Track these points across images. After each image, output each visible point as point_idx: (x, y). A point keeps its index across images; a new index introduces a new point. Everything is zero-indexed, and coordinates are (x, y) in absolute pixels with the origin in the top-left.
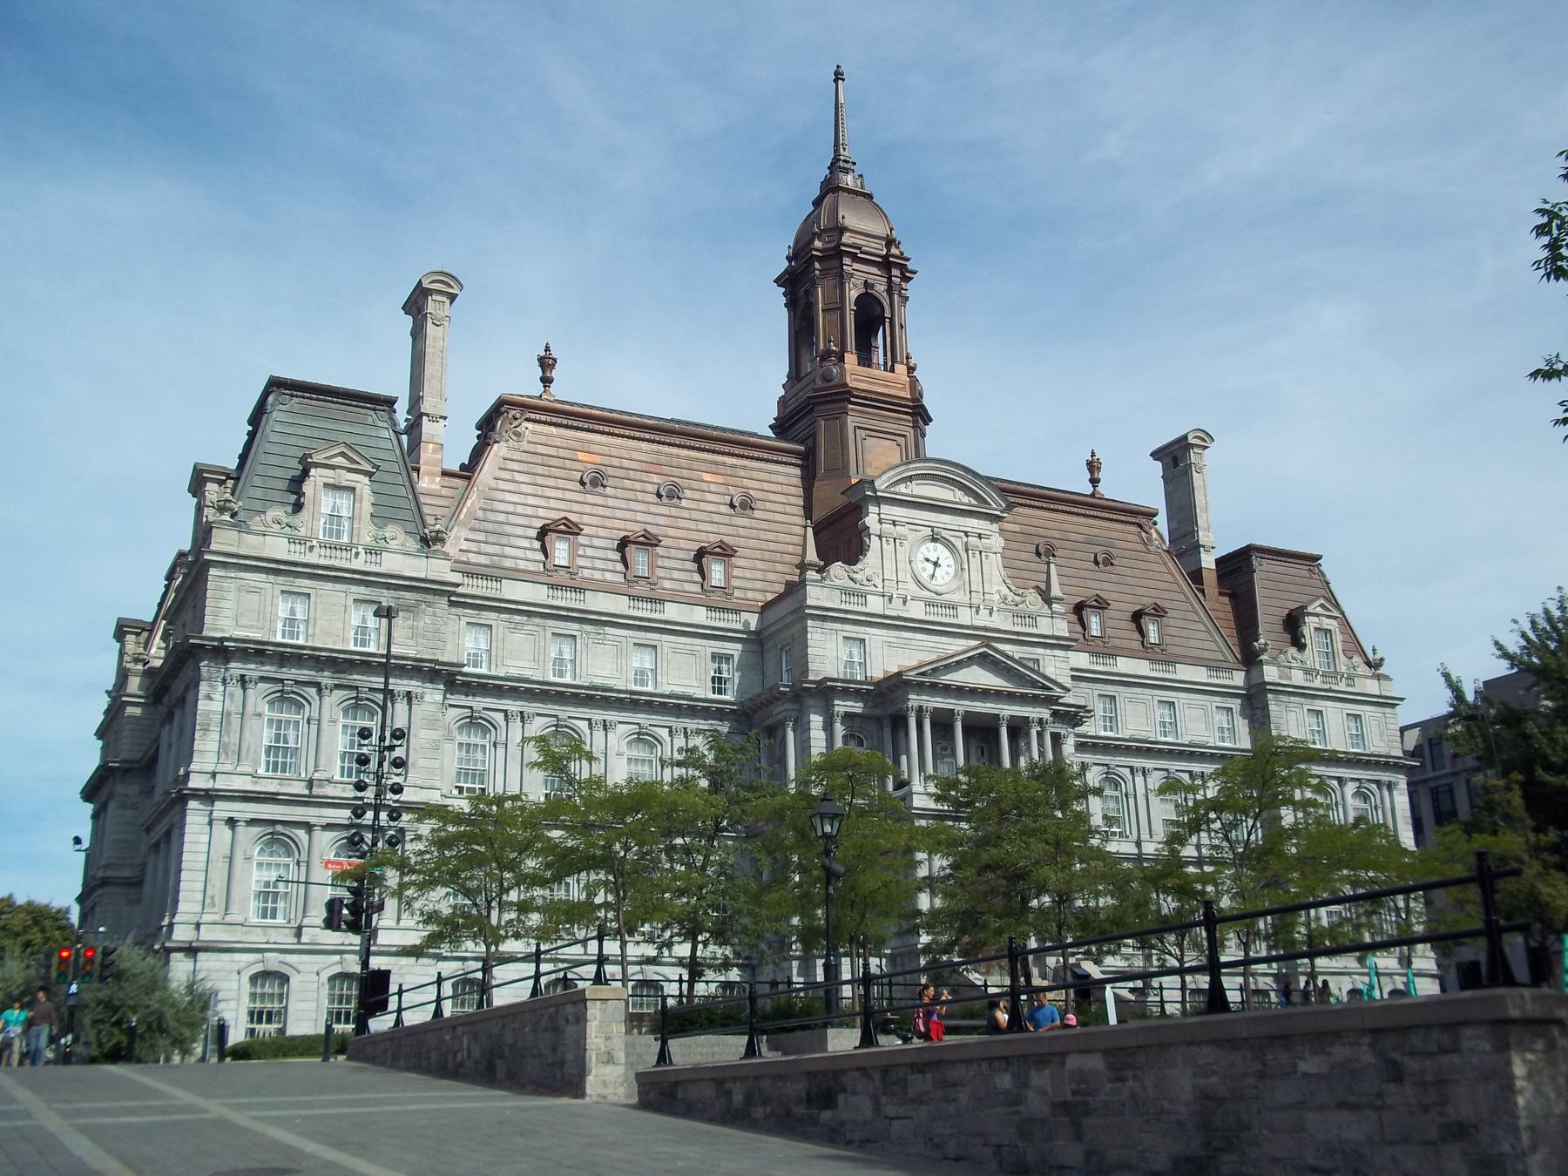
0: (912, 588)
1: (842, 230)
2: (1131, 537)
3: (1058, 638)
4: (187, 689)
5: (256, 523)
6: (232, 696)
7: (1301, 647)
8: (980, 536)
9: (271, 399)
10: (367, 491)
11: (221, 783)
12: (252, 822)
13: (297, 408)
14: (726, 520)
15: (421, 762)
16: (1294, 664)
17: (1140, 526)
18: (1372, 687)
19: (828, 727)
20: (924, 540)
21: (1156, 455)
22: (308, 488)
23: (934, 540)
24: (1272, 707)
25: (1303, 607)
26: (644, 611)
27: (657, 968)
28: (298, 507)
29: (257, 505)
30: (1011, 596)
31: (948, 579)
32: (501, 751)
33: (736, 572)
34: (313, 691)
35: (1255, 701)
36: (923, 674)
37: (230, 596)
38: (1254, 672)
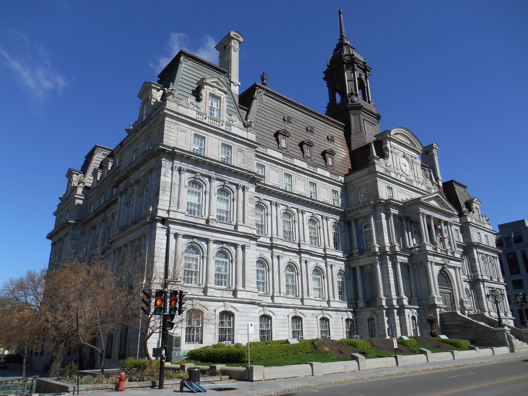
1: (353, 55)
4: (151, 171)
5: (183, 102)
6: (176, 176)
7: (473, 212)
9: (182, 58)
10: (225, 100)
11: (172, 215)
12: (185, 236)
13: (191, 65)
15: (249, 217)
17: (425, 170)
18: (487, 226)
19: (387, 218)
22: (203, 92)
23: (404, 157)
25: (473, 200)
26: (311, 169)
27: (328, 312)
28: (198, 100)
29: (181, 97)
31: (408, 171)
32: (269, 217)
33: (335, 162)
34: (207, 179)
37: (174, 131)
38: (463, 218)
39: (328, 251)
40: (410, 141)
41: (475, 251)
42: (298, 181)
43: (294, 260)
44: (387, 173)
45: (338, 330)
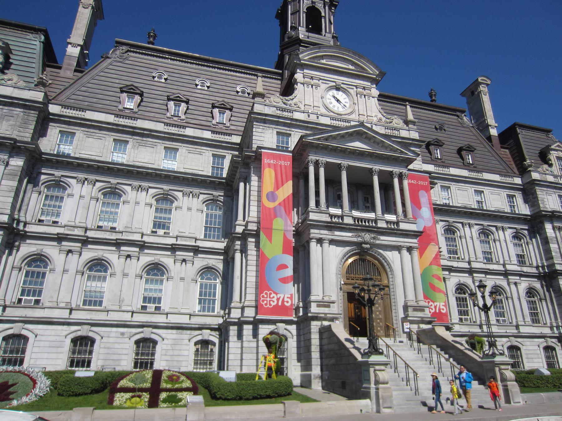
0: (323, 111)
2: (454, 121)
3: (413, 140)
7: (551, 165)
8: (364, 88)
14: (233, 97)
16: (547, 172)
17: (458, 116)
20: (331, 88)
21: (463, 94)
23: (338, 89)
24: (538, 192)
30: (384, 119)
35: (529, 192)
36: (319, 139)
38: (526, 176)
39: (182, 240)
40: (353, 64)
41: (548, 227)
42: (142, 149)
43: (105, 255)
44: (286, 114)
45: (176, 358)
